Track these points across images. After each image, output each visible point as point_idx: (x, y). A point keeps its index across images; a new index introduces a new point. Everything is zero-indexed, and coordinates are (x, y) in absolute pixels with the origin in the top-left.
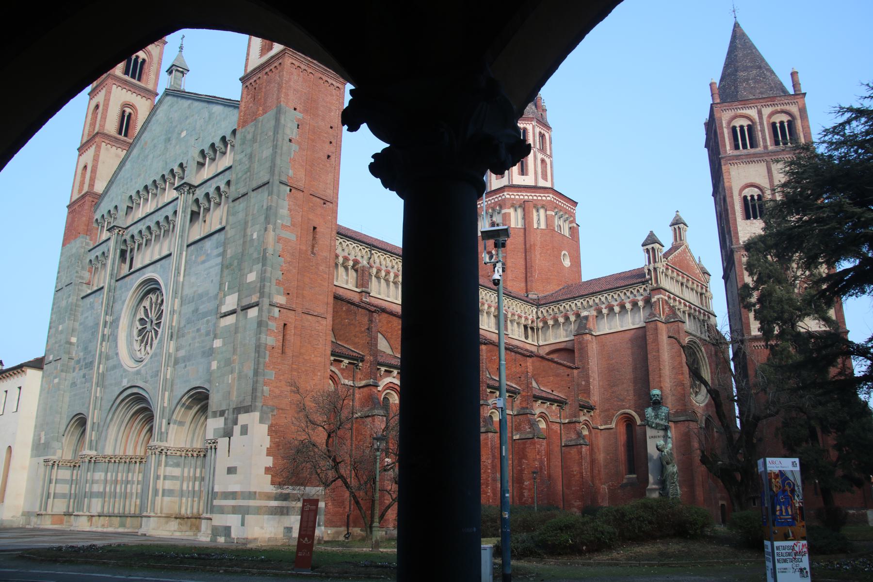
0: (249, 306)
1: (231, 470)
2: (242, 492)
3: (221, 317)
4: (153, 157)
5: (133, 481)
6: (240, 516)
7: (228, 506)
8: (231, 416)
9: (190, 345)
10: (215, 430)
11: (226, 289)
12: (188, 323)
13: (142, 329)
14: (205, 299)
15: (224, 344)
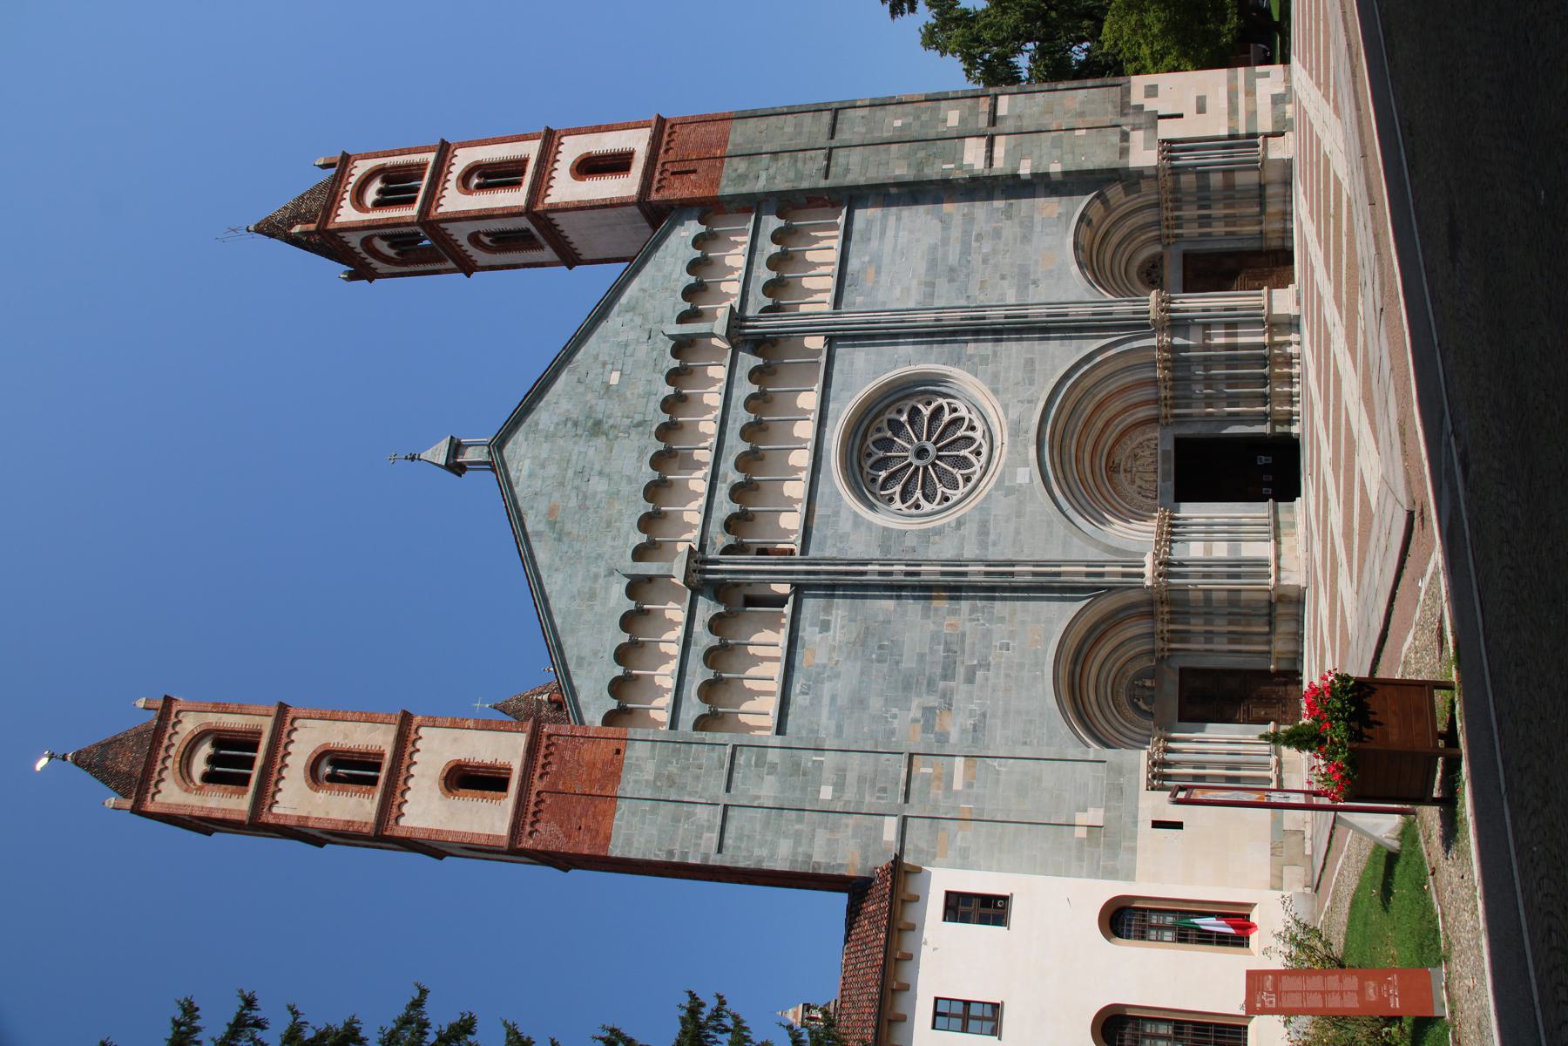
0: (992, 111)
1: (1201, 109)
2: (1229, 81)
3: (991, 165)
4: (600, 473)
5: (1205, 398)
6: (1257, 80)
7: (1247, 105)
8: (1130, 119)
9: (1003, 277)
10: (1145, 149)
11: (952, 166)
12: (966, 290)
13: (923, 487)
14: (940, 256)
15: (1030, 156)
